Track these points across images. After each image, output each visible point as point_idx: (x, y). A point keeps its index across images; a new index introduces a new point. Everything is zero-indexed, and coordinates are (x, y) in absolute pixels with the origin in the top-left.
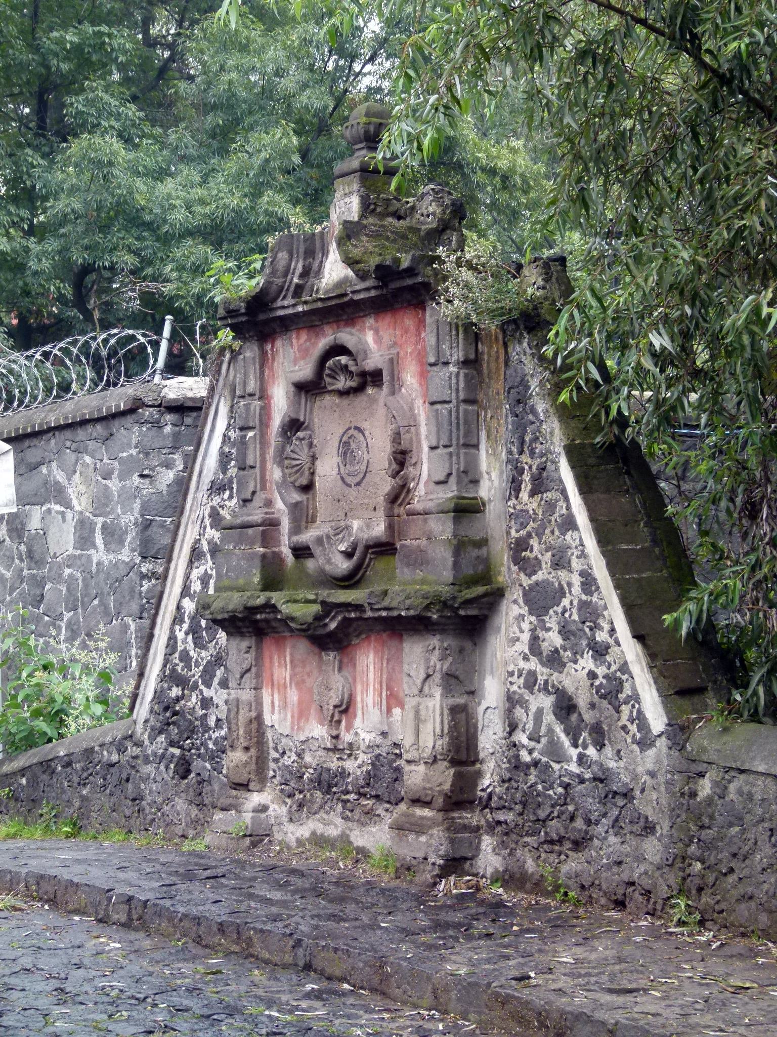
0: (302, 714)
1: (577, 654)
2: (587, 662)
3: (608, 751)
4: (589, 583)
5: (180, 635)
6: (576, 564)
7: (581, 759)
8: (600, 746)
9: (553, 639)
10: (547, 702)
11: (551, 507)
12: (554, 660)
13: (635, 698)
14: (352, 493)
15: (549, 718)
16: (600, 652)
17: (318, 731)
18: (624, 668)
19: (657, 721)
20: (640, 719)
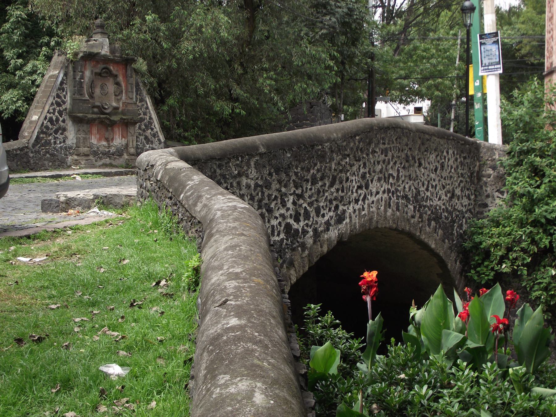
0: (100, 140)
1: (148, 129)
2: (150, 131)
3: (154, 145)
4: (151, 118)
5: (45, 122)
6: (148, 115)
7: (149, 147)
8: (152, 144)
9: (143, 127)
10: (143, 137)
11: (143, 105)
12: (144, 131)
13: (158, 136)
14: (104, 97)
15: (143, 140)
16: (152, 129)
17: (104, 143)
18: (157, 132)
19: (162, 139)
20: (159, 140)
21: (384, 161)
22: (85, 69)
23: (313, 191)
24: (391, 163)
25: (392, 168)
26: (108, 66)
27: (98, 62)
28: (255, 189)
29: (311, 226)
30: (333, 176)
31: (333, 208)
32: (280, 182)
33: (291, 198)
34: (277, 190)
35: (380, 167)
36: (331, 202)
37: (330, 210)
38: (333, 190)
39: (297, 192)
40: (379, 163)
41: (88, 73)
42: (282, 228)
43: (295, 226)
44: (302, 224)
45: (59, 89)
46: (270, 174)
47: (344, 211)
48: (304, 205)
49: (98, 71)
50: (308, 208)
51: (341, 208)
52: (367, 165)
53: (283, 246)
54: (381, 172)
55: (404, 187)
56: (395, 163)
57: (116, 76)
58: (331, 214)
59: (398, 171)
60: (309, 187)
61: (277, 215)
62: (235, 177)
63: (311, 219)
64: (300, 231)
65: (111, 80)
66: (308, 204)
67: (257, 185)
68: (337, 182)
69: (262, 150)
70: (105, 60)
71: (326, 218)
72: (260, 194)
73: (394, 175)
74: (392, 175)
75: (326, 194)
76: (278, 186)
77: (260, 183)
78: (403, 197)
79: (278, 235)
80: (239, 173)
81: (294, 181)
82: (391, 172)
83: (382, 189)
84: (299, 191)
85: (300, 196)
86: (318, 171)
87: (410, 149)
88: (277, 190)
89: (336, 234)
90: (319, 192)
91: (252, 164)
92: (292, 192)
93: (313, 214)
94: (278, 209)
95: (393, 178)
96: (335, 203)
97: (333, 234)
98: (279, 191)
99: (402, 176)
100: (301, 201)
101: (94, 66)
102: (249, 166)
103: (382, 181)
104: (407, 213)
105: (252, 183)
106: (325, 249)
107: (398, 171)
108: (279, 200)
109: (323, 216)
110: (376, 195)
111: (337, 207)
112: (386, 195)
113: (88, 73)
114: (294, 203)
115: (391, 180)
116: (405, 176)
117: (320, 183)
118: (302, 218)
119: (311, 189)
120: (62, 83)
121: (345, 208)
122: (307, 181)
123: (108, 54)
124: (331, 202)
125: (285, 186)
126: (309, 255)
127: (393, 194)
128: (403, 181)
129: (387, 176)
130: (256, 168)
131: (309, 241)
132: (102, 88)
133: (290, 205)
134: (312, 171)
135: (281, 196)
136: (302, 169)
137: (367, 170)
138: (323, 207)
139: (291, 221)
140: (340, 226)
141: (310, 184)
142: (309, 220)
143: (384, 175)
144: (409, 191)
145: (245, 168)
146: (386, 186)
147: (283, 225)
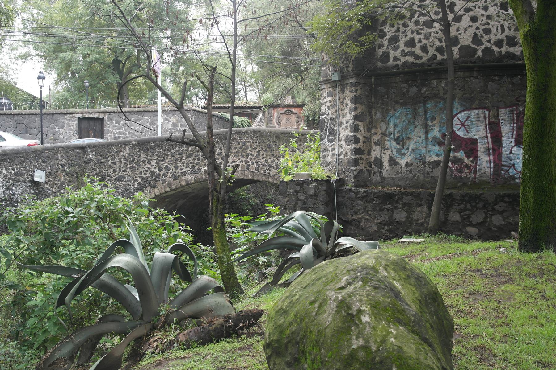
21: (241, 148)
22: (274, 112)
23: (172, 159)
24: (250, 149)
25: (250, 151)
26: (290, 109)
27: (283, 107)
28: (128, 157)
29: (171, 173)
30: (189, 153)
31: (190, 167)
32: (147, 155)
33: (155, 161)
34: (145, 158)
35: (236, 150)
36: (188, 164)
37: (187, 167)
38: (189, 159)
39: (159, 159)
40: (235, 148)
41: (276, 114)
42: (148, 172)
43: (158, 172)
44: (164, 171)
45: (259, 122)
46: (139, 151)
47: (199, 169)
48: (165, 165)
49: (283, 112)
50: (169, 166)
51: (197, 167)
52: (223, 149)
53: (149, 179)
54: (237, 152)
55: (266, 161)
56: (256, 148)
57: (296, 114)
58: (189, 169)
59: (259, 152)
60: (169, 157)
61: (144, 167)
62: (116, 152)
63: (171, 170)
64: (162, 174)
65: (294, 116)
66: (169, 164)
67: (129, 156)
68: (194, 156)
69: (134, 143)
70: (288, 106)
71: (183, 171)
72: (131, 159)
73: (253, 154)
74: (251, 154)
75: (183, 161)
76: (145, 156)
77: (132, 154)
78: (264, 165)
79: (145, 174)
80: (118, 151)
81: (157, 155)
82: (250, 153)
83: (241, 160)
84: (162, 159)
85: (161, 161)
86: (177, 151)
87: (273, 142)
88: (145, 158)
89: (192, 178)
90: (177, 160)
91: (127, 148)
92: (155, 158)
93: (172, 168)
94: (145, 165)
95: (253, 156)
96: (191, 165)
97: (190, 178)
98: (147, 158)
99: (263, 155)
100: (162, 163)
101: (281, 110)
102: (125, 148)
103: (240, 157)
104: (269, 173)
105: (127, 155)
106: (183, 183)
107: (259, 152)
108: (147, 162)
109: (181, 169)
110: (231, 163)
111: (193, 167)
112: (244, 163)
113: (276, 114)
114: (156, 163)
115: (250, 156)
116: (267, 155)
117: (178, 156)
118: (163, 169)
119: (170, 158)
120: (261, 119)
121: (202, 167)
122: (168, 155)
123: (291, 103)
124: (188, 164)
125: (150, 156)
126: (168, 184)
127: (252, 163)
128: (264, 158)
129: (244, 154)
130: (129, 149)
131: (170, 178)
132: (287, 120)
133: (154, 163)
134: (172, 151)
135: (149, 160)
136: (163, 150)
137: (223, 151)
138: (180, 166)
139: (157, 170)
140: (196, 174)
141: (170, 156)
142: (169, 170)
143: (242, 154)
144: (272, 162)
145: (122, 149)
146: (244, 160)
147: (149, 171)
